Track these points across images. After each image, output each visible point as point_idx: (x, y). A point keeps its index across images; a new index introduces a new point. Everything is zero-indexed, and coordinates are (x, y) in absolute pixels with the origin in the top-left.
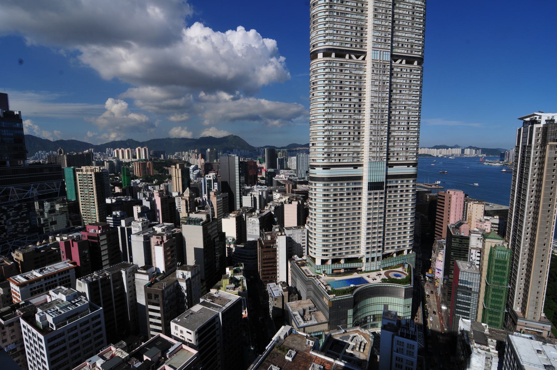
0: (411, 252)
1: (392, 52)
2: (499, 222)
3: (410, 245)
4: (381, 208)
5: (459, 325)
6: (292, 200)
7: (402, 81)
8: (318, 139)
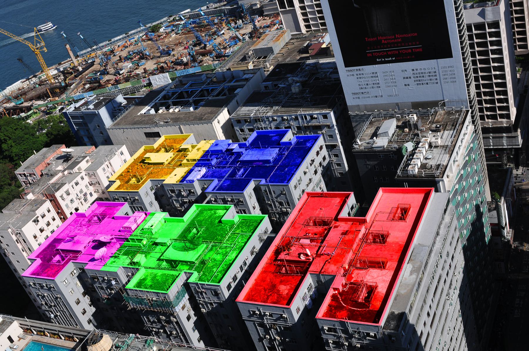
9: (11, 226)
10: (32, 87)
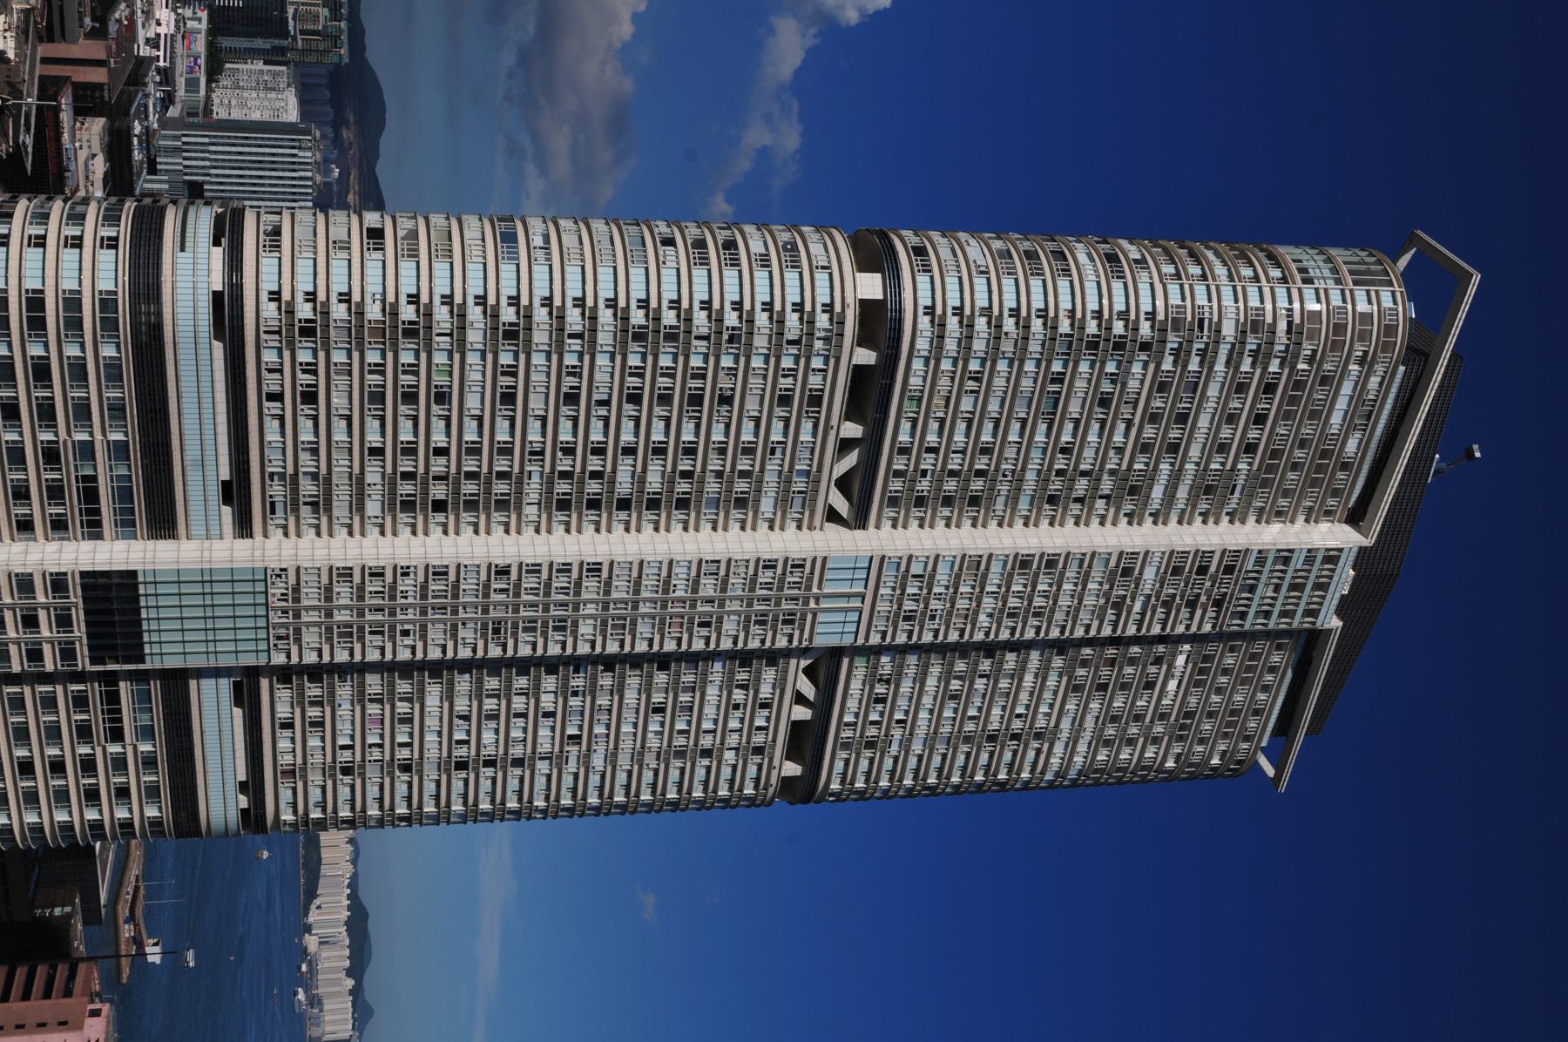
1: (854, 651)
7: (710, 711)
8: (407, 267)
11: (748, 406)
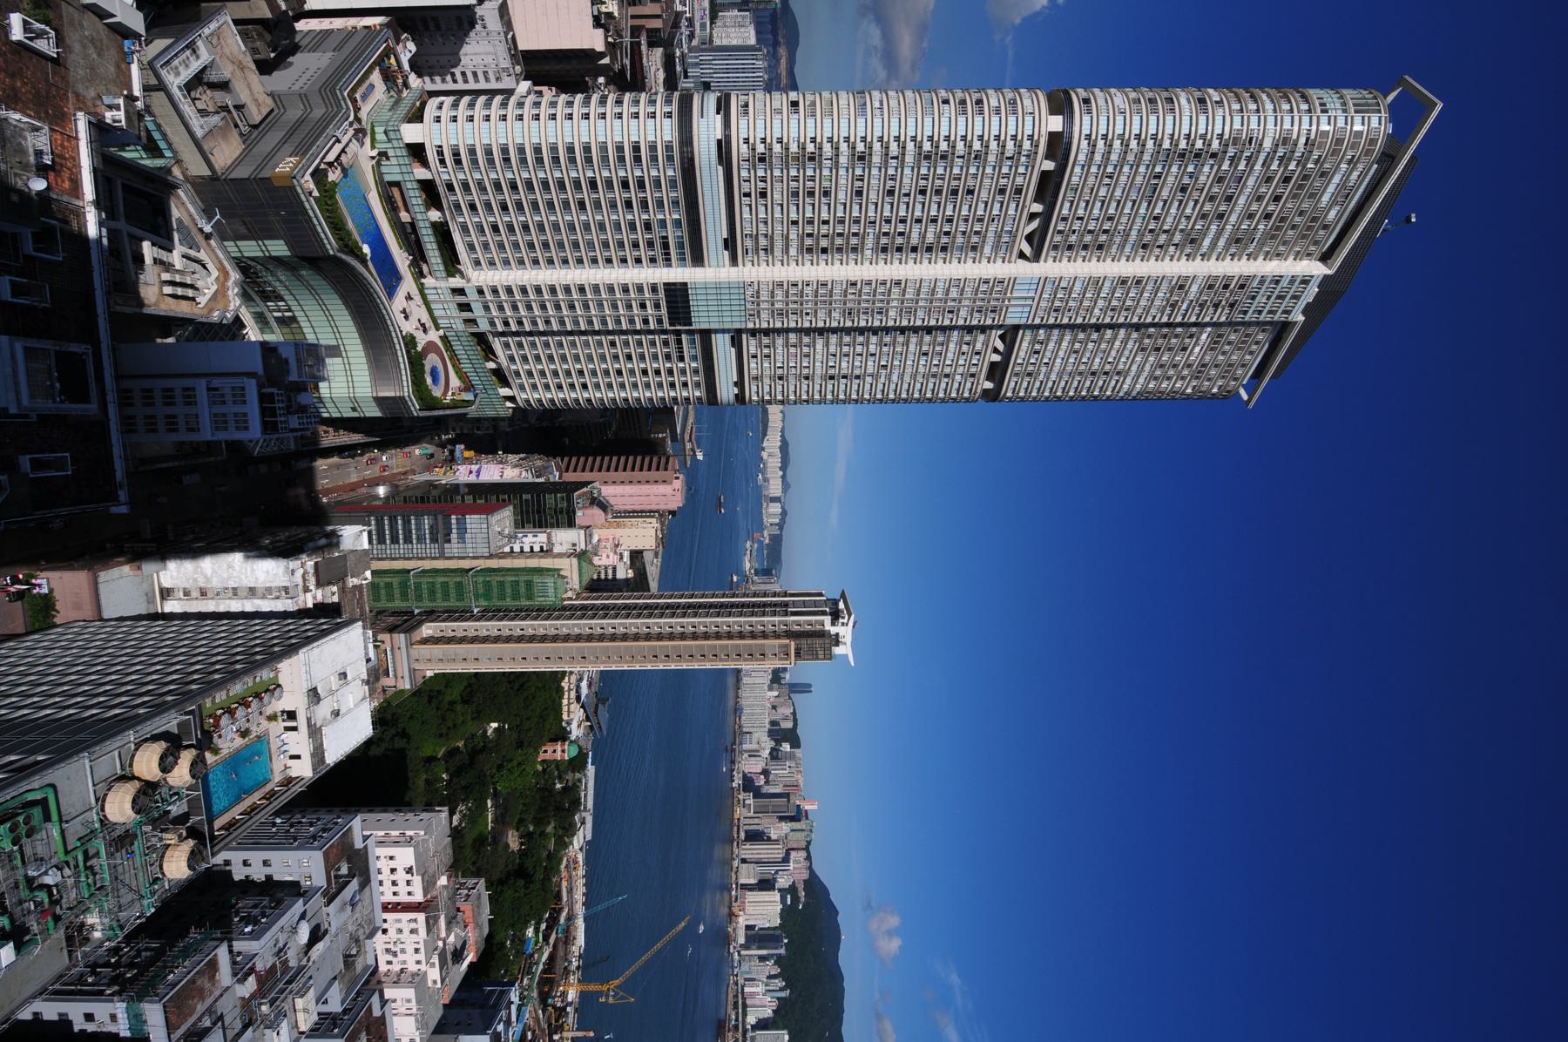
0: (509, 404)
2: (620, 580)
3: (527, 401)
4: (618, 322)
5: (347, 527)
6: (607, 30)
7: (950, 355)
8: (810, 122)
9: (426, 837)
10: (569, 957)
11: (982, 195)
